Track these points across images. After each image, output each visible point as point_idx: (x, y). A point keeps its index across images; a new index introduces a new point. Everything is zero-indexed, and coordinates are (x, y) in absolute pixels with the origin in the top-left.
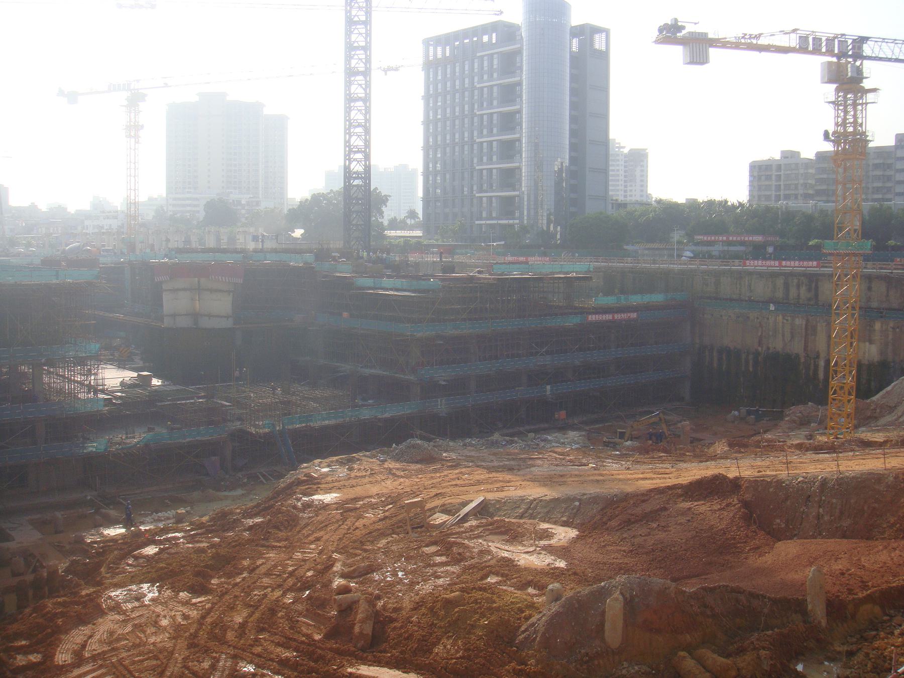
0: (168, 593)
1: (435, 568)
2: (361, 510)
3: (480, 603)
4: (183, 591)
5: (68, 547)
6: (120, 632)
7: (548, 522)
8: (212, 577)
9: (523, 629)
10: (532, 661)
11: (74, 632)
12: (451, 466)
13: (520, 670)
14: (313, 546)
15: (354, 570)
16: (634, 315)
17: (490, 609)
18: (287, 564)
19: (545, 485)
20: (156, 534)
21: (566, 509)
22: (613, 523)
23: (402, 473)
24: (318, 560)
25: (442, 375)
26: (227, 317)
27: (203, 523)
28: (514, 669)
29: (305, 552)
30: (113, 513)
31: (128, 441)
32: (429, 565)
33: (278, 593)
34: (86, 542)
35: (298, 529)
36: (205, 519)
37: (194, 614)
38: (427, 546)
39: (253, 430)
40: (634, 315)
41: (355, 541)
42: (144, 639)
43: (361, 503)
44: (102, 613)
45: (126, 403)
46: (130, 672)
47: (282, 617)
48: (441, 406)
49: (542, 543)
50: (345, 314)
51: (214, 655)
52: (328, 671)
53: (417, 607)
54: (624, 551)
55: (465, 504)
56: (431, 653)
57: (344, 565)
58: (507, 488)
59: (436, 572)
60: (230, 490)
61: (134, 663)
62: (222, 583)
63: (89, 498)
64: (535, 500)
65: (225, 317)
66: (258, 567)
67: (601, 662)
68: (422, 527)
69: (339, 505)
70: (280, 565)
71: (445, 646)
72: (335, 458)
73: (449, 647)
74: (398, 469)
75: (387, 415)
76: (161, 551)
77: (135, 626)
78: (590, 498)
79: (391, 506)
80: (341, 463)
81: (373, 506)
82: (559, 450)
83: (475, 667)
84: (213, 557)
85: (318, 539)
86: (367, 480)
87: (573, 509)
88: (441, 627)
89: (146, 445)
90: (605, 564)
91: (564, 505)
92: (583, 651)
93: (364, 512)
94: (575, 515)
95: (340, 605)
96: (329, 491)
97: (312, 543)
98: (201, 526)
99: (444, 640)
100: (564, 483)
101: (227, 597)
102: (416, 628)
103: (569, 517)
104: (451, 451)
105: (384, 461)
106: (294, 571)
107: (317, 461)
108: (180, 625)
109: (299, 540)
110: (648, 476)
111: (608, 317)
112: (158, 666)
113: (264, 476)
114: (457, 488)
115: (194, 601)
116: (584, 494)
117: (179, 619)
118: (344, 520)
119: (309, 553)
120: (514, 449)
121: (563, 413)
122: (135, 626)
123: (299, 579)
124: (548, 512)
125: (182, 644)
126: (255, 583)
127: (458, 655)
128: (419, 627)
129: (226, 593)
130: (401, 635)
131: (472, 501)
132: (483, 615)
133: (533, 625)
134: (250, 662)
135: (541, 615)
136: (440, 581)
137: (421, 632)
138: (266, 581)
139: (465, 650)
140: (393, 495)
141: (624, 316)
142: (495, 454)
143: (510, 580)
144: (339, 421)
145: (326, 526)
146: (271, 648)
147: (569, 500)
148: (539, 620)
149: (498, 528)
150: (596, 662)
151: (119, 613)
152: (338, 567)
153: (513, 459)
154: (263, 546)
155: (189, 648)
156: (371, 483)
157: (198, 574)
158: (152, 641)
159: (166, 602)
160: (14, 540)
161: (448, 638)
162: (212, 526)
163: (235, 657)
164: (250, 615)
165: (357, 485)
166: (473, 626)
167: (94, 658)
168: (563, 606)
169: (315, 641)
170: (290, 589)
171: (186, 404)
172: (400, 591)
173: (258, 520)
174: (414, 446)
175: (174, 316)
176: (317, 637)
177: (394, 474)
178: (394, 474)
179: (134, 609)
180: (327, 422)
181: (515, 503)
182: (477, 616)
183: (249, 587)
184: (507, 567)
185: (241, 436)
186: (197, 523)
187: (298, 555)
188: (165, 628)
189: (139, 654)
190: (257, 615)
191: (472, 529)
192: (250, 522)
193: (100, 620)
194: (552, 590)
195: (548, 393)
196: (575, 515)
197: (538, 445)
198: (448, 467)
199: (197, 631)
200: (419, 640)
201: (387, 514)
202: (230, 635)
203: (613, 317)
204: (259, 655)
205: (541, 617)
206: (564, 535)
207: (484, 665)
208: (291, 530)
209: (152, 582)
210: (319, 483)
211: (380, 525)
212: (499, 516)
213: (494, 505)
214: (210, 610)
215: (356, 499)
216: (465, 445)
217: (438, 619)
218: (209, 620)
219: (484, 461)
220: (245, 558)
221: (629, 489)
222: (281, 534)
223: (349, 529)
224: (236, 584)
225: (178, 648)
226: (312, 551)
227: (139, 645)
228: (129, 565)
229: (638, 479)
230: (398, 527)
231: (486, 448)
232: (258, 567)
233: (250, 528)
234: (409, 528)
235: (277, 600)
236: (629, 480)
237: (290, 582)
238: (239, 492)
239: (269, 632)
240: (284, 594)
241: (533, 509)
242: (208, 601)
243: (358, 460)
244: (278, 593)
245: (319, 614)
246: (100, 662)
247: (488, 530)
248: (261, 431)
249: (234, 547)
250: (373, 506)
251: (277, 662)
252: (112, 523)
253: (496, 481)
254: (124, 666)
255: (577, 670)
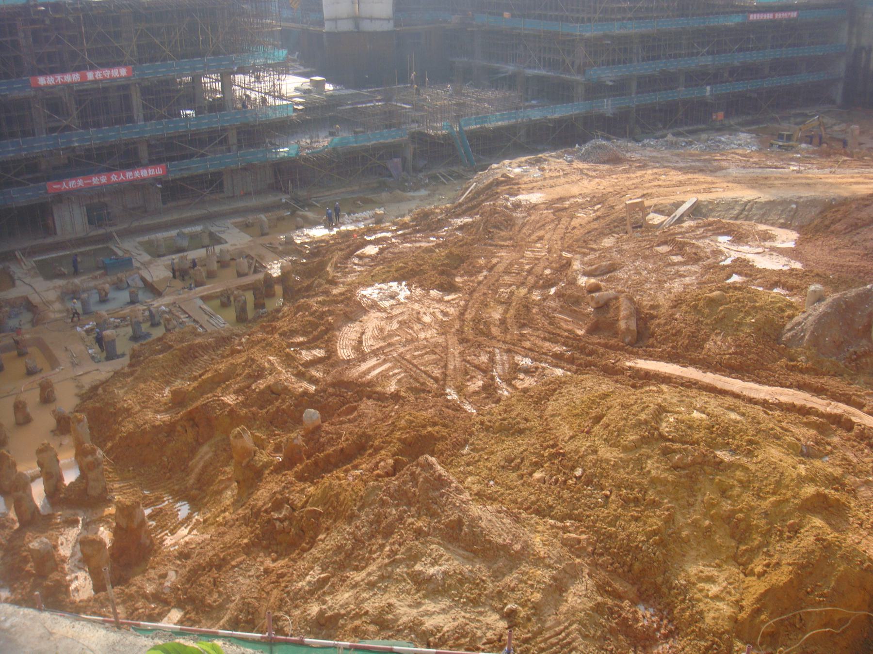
0: (419, 291)
1: (676, 267)
2: (571, 210)
3: (743, 302)
4: (433, 289)
5: (281, 248)
6: (388, 328)
7: (765, 224)
8: (455, 276)
9: (788, 327)
10: (802, 358)
11: (346, 329)
12: (639, 167)
13: (793, 366)
14: (539, 245)
15: (596, 269)
16: (794, 14)
17: (754, 307)
18: (522, 263)
19: (753, 188)
20: (364, 234)
21: (782, 211)
22: (838, 226)
23: (594, 174)
24: (551, 259)
25: (608, 75)
26: (388, 20)
27: (406, 223)
28: (787, 366)
29: (534, 251)
30: (310, 215)
31: (315, 145)
32: (669, 265)
33: (523, 291)
34: (296, 244)
35: (517, 228)
36: (407, 219)
37: (451, 310)
38: (658, 245)
39: (431, 132)
40: (794, 14)
41: (577, 241)
42: (415, 335)
43: (568, 203)
44: (365, 311)
45: (309, 108)
46: (415, 366)
47: (537, 314)
48: (608, 106)
49: (768, 244)
50: (507, 15)
51: (488, 349)
52: (606, 365)
53: (677, 303)
54: (859, 254)
55: (678, 205)
56: (703, 348)
57: (582, 263)
58: (714, 190)
59: (678, 271)
60: (415, 191)
61: (415, 357)
62: (465, 281)
63: (284, 201)
64: (749, 201)
65: (385, 19)
66: (495, 265)
67: (869, 360)
68: (641, 227)
69: (549, 205)
70: (516, 264)
71: (715, 343)
72: (523, 159)
73: (719, 343)
74: (588, 169)
75: (557, 116)
76: (382, 251)
77: (399, 322)
78: (807, 201)
79: (599, 206)
80: (531, 164)
81: (581, 206)
82: (740, 151)
83: (749, 362)
84: (448, 257)
85: (541, 238)
86: (562, 180)
87: (790, 211)
88: (707, 324)
89: (334, 149)
90: (842, 266)
91: (780, 208)
92: (851, 350)
93: (575, 211)
94: (793, 217)
95: (598, 303)
96: (531, 190)
97: (536, 242)
98: (404, 226)
99: (713, 337)
100: (771, 186)
101: (476, 295)
102: (683, 325)
103: (786, 219)
104: (635, 151)
105: (571, 162)
106: (533, 268)
107: (507, 162)
108: (442, 321)
109: (523, 239)
110: (861, 180)
111: (769, 16)
112: (440, 360)
113: (443, 176)
114: (661, 189)
115: (446, 298)
116: (800, 197)
117: (440, 316)
118: (559, 220)
119: (538, 252)
120: (695, 149)
121: (721, 115)
122: (399, 322)
123: (540, 277)
124: (764, 214)
125: (453, 340)
126: (497, 281)
127: (730, 351)
128: (686, 324)
129: (474, 290)
130: (667, 331)
131: (684, 202)
132: (748, 314)
133: (799, 324)
134: (526, 356)
135: (806, 315)
136: (687, 280)
137: (689, 328)
138: (507, 278)
139: (737, 346)
140: (597, 195)
141: (784, 15)
142: (678, 155)
143: (756, 279)
144: (513, 121)
145: (543, 225)
146: (539, 343)
147: (784, 202)
148: (805, 319)
149: (718, 228)
150: (864, 360)
151: (379, 311)
152: (577, 265)
153: (699, 161)
154: (491, 245)
155: (460, 343)
156: (567, 182)
157: (442, 273)
158: (423, 337)
159: (420, 300)
160: (226, 242)
161: (717, 334)
162: (416, 226)
163: (509, 351)
164: (506, 311)
165: (556, 185)
166: (740, 324)
167: (375, 353)
168: (831, 307)
169: (578, 335)
170: (534, 287)
171: (366, 108)
172: (651, 289)
173: (467, 220)
174: (599, 147)
175: (335, 20)
176: (580, 332)
177: (586, 175)
178: (586, 175)
179: (392, 307)
180: (500, 123)
181: (729, 204)
182: (742, 315)
183: (493, 284)
184: (742, 266)
185: (419, 138)
186: (401, 223)
187: (528, 254)
188: (430, 325)
189: (417, 349)
190: (512, 312)
191: (692, 229)
192: (459, 221)
193: (365, 318)
194: (815, 291)
195: (708, 94)
196: (793, 217)
197: (718, 146)
198: (636, 167)
199: (462, 327)
200: (689, 336)
201: (598, 213)
202: (495, 331)
203: (774, 16)
204: (530, 350)
205: (807, 317)
206: (787, 238)
207: (758, 360)
208: (511, 230)
209: (399, 280)
210: (518, 184)
211: (595, 225)
212: (714, 217)
213: (706, 206)
214: (465, 308)
215: (562, 199)
216: (644, 146)
217: (703, 316)
218: (468, 316)
219: (669, 162)
220: (479, 257)
221: (845, 193)
222: (502, 233)
223: (567, 228)
224: (480, 283)
225: (450, 343)
226: (540, 250)
227: (412, 341)
228: (355, 264)
229: (851, 184)
230: (615, 227)
231: (666, 149)
232: (495, 265)
233: (461, 228)
234: (629, 228)
235: (525, 297)
236: (840, 183)
237: (531, 280)
238: (423, 192)
239: (531, 327)
240: (530, 291)
241: (746, 210)
242: (460, 299)
243: (545, 160)
244: (523, 291)
245: (575, 311)
246: (383, 357)
247: (710, 230)
248: (439, 132)
249: (461, 246)
250: (581, 206)
251: (551, 356)
252: (313, 224)
253: (699, 182)
254: (405, 360)
255: (846, 367)
